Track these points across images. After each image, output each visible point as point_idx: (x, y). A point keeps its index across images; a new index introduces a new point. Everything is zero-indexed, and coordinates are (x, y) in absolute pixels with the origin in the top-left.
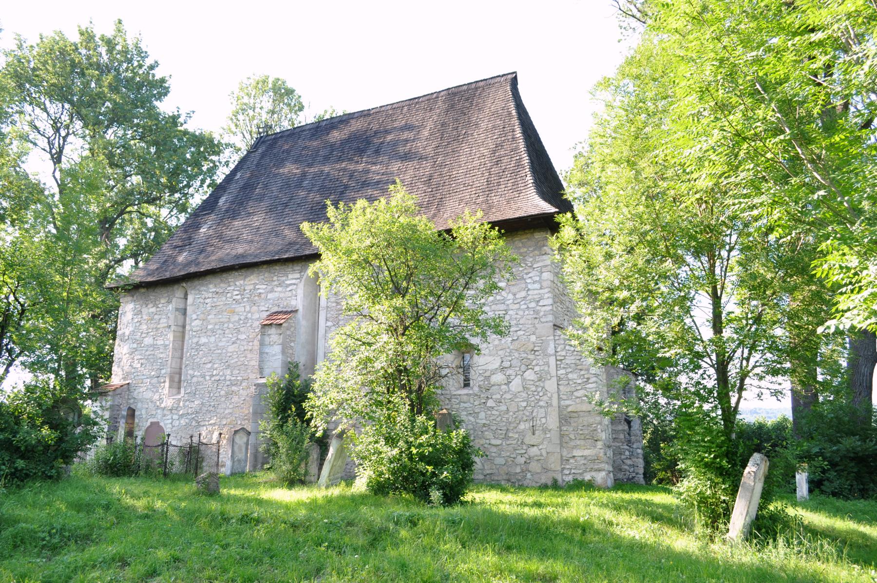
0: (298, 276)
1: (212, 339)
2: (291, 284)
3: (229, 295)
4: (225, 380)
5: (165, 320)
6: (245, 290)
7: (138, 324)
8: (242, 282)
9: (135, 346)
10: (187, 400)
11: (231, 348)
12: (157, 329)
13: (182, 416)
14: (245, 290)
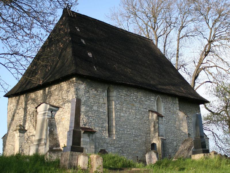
0: (154, 98)
1: (126, 115)
2: (152, 101)
3: (131, 97)
4: (132, 134)
5: (102, 100)
6: (138, 97)
7: (88, 97)
8: (136, 93)
9: (88, 109)
10: (118, 141)
11: (134, 121)
12: (99, 103)
13: (116, 148)
14: (138, 97)
